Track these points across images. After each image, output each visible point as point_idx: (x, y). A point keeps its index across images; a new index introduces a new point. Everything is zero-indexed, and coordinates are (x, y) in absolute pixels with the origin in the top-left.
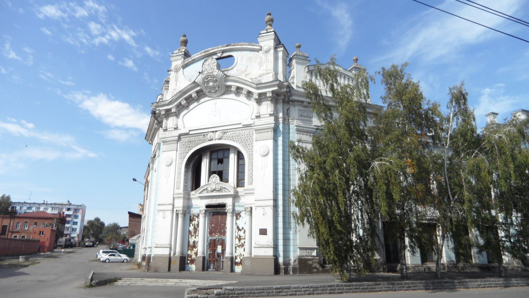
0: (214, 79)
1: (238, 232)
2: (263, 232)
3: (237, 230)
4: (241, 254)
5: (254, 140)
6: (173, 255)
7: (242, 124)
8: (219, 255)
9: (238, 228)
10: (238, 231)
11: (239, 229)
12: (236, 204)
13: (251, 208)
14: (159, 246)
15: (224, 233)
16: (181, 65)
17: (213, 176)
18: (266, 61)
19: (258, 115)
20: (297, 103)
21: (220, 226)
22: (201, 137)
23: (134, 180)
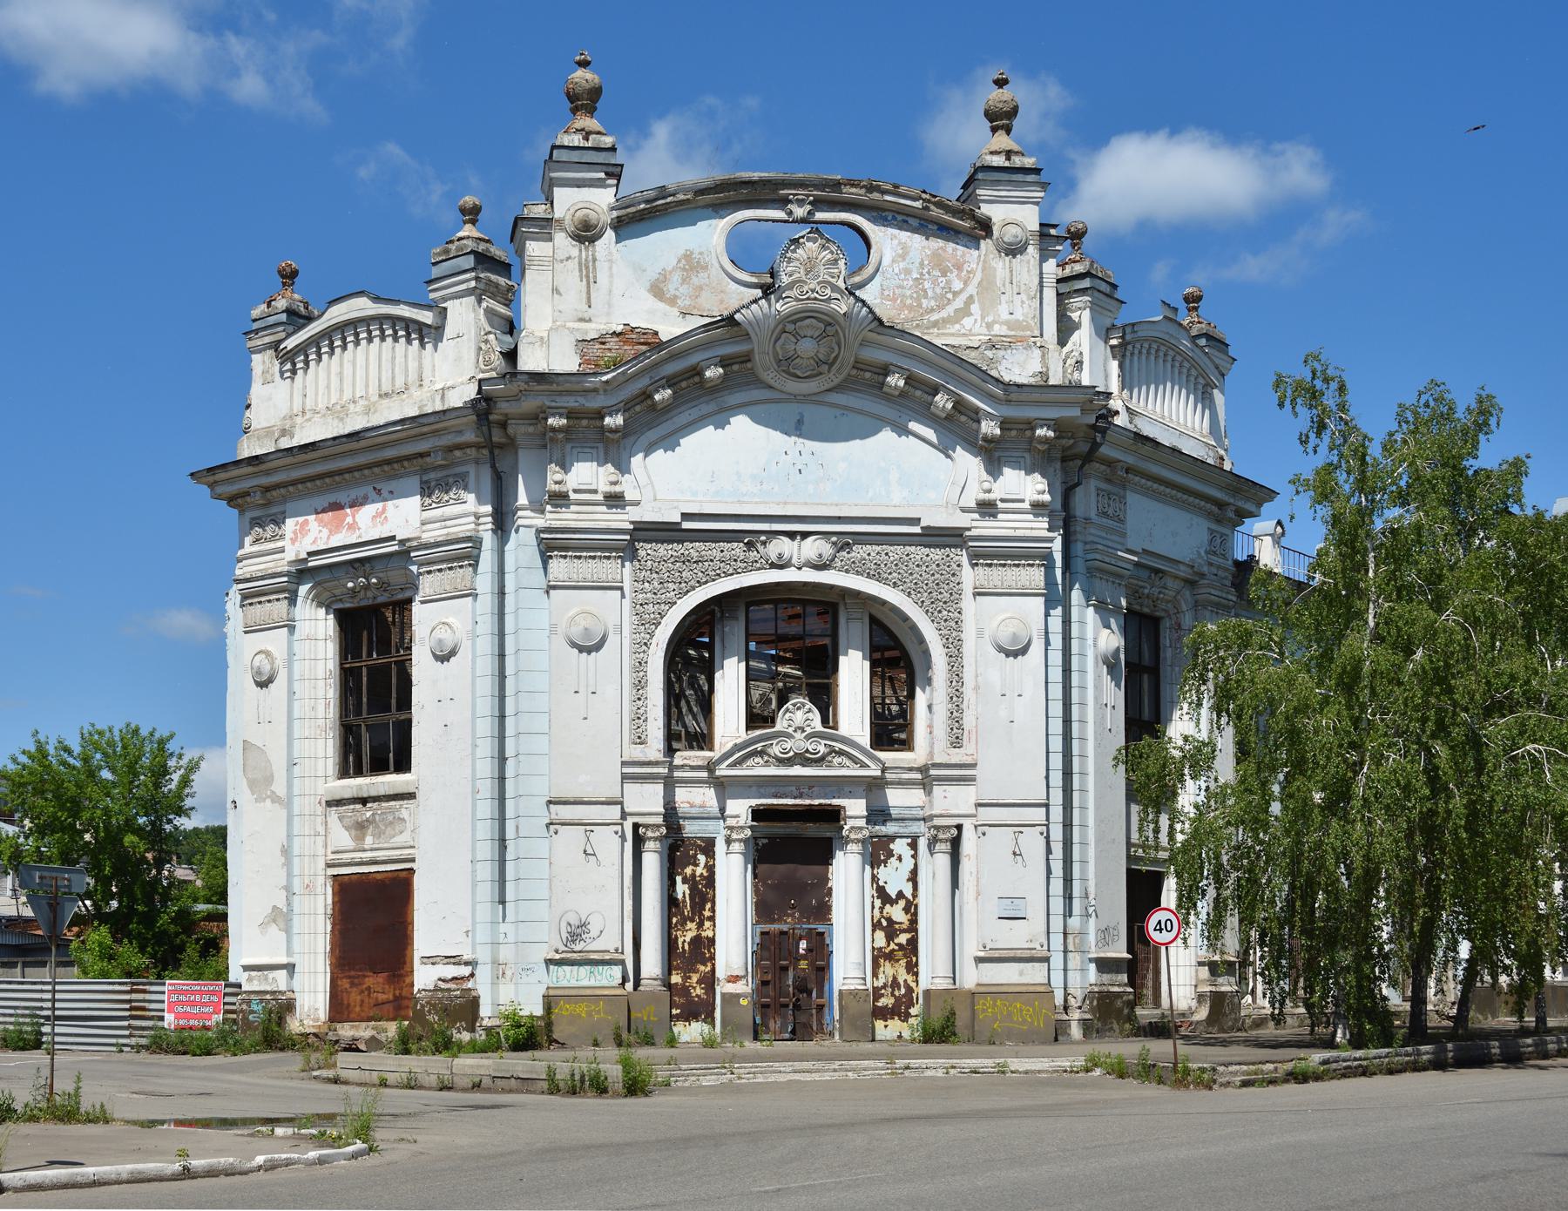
1: (882, 909)
3: (878, 903)
9: (882, 893)
10: (884, 904)
22: (737, 549)
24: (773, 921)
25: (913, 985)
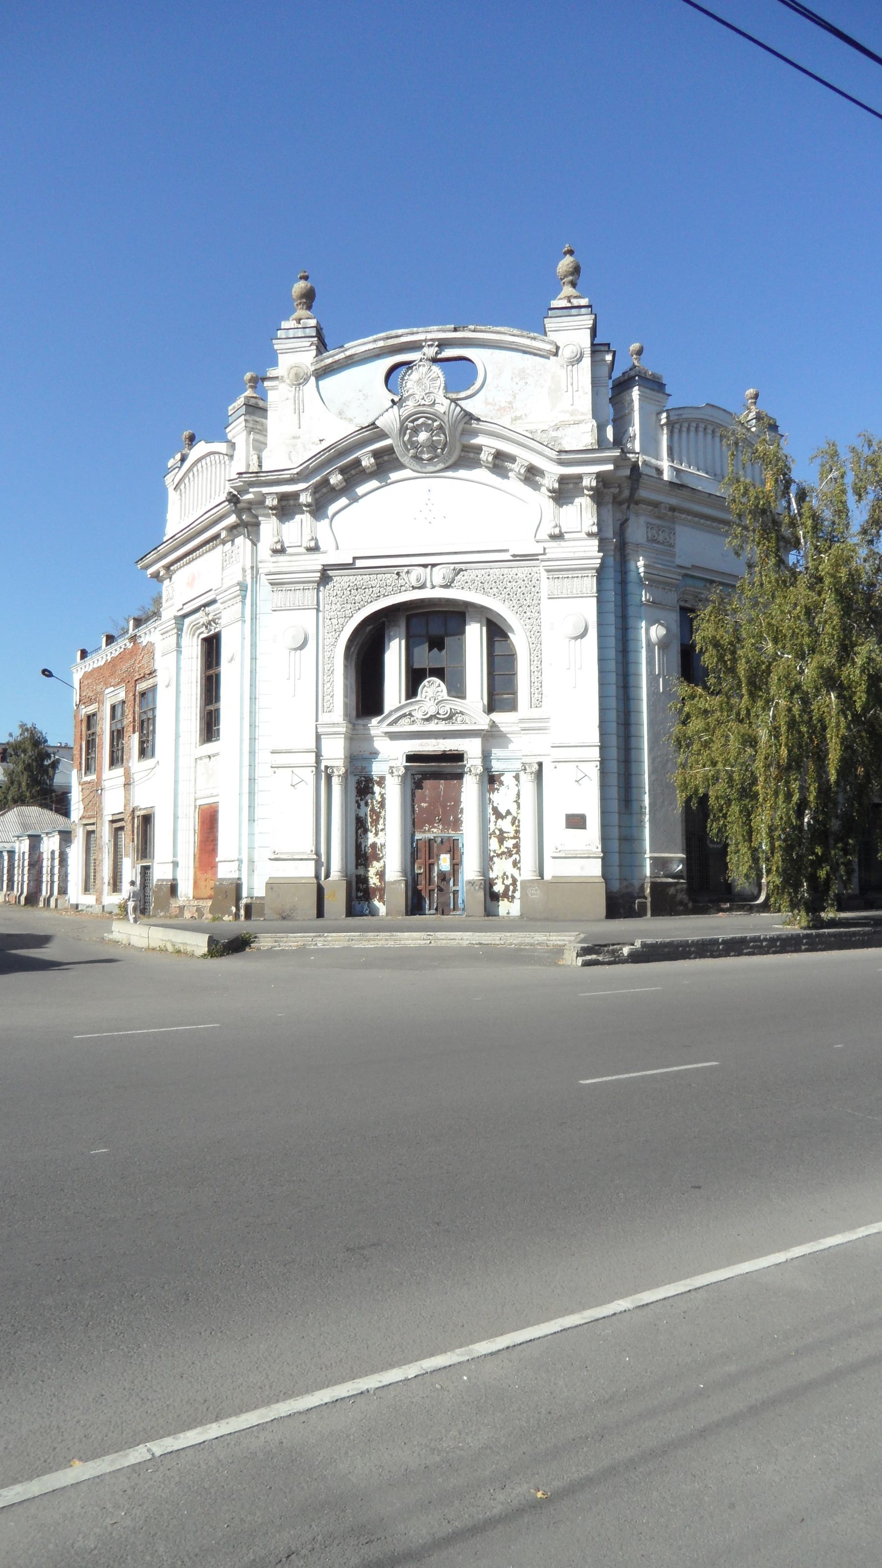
0: (436, 424)
2: (576, 822)
4: (505, 874)
5: (544, 595)
6: (325, 879)
7: (512, 552)
8: (443, 877)
9: (496, 811)
10: (497, 818)
11: (498, 815)
12: (496, 752)
13: (540, 765)
14: (283, 857)
15: (457, 824)
16: (313, 368)
17: (429, 682)
18: (570, 386)
19: (557, 531)
20: (644, 506)
21: (444, 807)
22: (391, 578)
23: (47, 673)
24: (425, 832)
25: (516, 876)
